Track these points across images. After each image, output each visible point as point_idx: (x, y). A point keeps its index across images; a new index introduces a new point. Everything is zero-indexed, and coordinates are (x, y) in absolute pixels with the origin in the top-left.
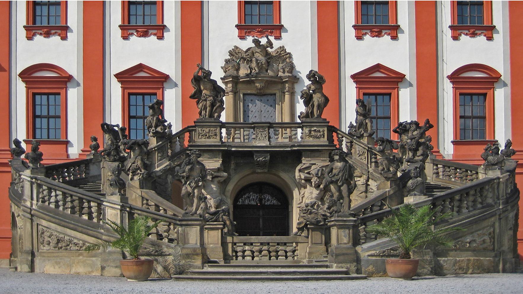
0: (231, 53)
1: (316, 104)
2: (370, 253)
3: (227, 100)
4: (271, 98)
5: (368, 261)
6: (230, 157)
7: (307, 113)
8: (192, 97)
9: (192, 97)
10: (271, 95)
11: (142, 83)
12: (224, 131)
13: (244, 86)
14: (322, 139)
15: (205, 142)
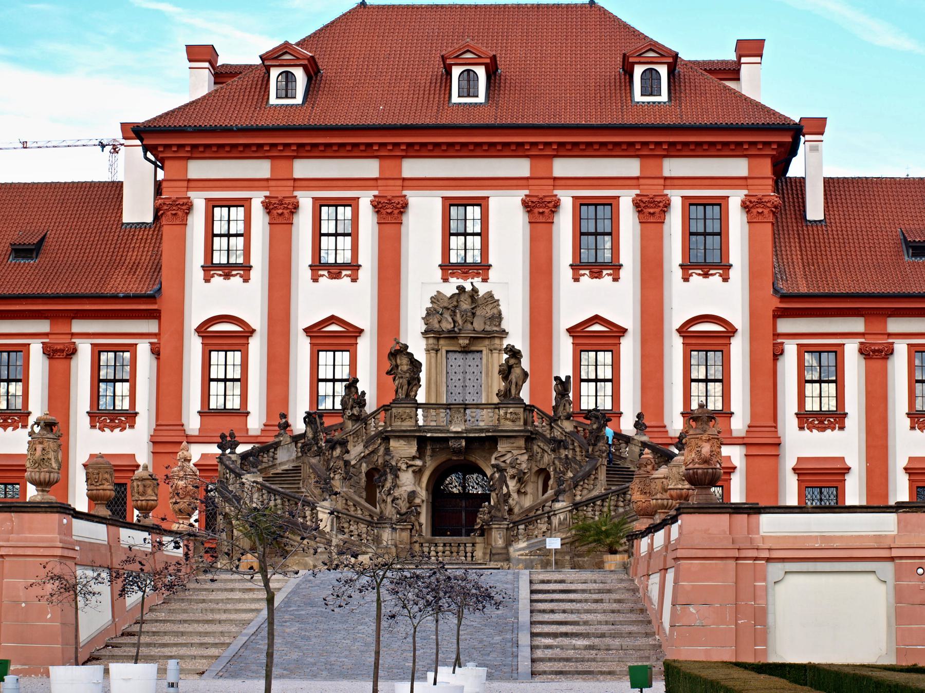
0: (432, 302)
1: (514, 381)
2: (522, 552)
3: (423, 375)
4: (477, 355)
5: (518, 560)
6: (424, 442)
7: (506, 389)
8: (388, 373)
9: (388, 373)
10: (478, 352)
11: (333, 336)
12: (420, 411)
13: (447, 342)
14: (517, 423)
15: (401, 426)
